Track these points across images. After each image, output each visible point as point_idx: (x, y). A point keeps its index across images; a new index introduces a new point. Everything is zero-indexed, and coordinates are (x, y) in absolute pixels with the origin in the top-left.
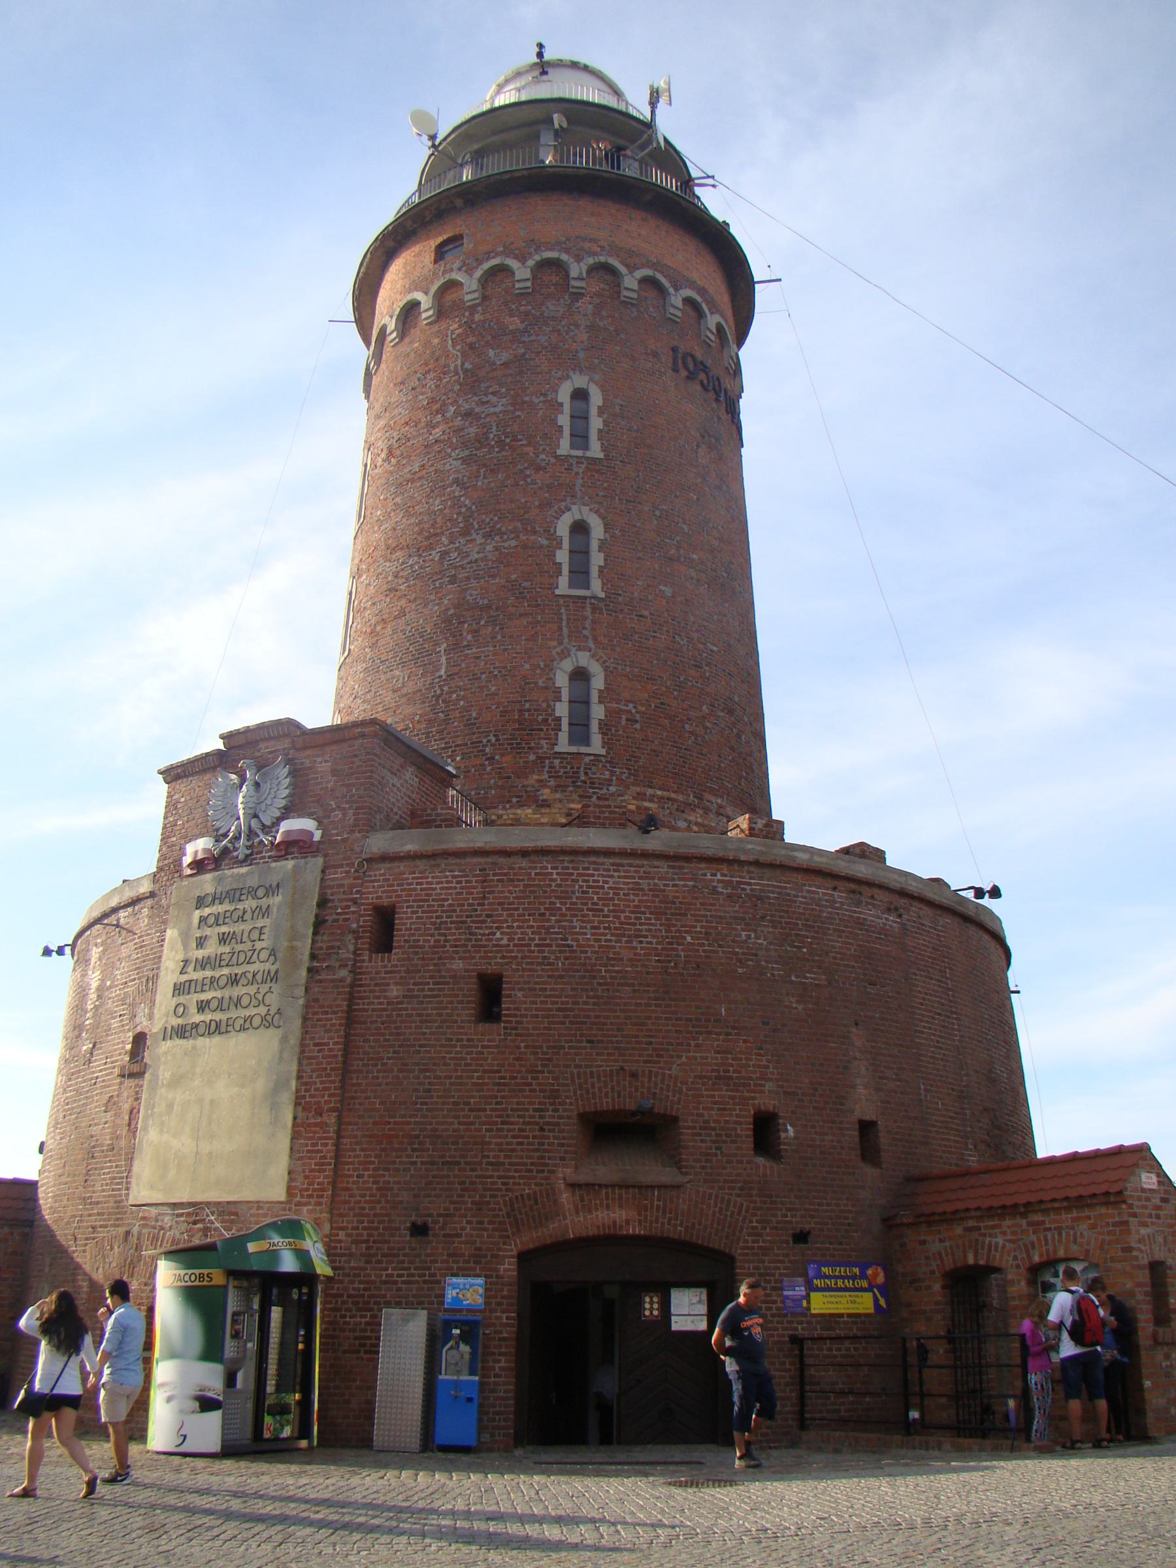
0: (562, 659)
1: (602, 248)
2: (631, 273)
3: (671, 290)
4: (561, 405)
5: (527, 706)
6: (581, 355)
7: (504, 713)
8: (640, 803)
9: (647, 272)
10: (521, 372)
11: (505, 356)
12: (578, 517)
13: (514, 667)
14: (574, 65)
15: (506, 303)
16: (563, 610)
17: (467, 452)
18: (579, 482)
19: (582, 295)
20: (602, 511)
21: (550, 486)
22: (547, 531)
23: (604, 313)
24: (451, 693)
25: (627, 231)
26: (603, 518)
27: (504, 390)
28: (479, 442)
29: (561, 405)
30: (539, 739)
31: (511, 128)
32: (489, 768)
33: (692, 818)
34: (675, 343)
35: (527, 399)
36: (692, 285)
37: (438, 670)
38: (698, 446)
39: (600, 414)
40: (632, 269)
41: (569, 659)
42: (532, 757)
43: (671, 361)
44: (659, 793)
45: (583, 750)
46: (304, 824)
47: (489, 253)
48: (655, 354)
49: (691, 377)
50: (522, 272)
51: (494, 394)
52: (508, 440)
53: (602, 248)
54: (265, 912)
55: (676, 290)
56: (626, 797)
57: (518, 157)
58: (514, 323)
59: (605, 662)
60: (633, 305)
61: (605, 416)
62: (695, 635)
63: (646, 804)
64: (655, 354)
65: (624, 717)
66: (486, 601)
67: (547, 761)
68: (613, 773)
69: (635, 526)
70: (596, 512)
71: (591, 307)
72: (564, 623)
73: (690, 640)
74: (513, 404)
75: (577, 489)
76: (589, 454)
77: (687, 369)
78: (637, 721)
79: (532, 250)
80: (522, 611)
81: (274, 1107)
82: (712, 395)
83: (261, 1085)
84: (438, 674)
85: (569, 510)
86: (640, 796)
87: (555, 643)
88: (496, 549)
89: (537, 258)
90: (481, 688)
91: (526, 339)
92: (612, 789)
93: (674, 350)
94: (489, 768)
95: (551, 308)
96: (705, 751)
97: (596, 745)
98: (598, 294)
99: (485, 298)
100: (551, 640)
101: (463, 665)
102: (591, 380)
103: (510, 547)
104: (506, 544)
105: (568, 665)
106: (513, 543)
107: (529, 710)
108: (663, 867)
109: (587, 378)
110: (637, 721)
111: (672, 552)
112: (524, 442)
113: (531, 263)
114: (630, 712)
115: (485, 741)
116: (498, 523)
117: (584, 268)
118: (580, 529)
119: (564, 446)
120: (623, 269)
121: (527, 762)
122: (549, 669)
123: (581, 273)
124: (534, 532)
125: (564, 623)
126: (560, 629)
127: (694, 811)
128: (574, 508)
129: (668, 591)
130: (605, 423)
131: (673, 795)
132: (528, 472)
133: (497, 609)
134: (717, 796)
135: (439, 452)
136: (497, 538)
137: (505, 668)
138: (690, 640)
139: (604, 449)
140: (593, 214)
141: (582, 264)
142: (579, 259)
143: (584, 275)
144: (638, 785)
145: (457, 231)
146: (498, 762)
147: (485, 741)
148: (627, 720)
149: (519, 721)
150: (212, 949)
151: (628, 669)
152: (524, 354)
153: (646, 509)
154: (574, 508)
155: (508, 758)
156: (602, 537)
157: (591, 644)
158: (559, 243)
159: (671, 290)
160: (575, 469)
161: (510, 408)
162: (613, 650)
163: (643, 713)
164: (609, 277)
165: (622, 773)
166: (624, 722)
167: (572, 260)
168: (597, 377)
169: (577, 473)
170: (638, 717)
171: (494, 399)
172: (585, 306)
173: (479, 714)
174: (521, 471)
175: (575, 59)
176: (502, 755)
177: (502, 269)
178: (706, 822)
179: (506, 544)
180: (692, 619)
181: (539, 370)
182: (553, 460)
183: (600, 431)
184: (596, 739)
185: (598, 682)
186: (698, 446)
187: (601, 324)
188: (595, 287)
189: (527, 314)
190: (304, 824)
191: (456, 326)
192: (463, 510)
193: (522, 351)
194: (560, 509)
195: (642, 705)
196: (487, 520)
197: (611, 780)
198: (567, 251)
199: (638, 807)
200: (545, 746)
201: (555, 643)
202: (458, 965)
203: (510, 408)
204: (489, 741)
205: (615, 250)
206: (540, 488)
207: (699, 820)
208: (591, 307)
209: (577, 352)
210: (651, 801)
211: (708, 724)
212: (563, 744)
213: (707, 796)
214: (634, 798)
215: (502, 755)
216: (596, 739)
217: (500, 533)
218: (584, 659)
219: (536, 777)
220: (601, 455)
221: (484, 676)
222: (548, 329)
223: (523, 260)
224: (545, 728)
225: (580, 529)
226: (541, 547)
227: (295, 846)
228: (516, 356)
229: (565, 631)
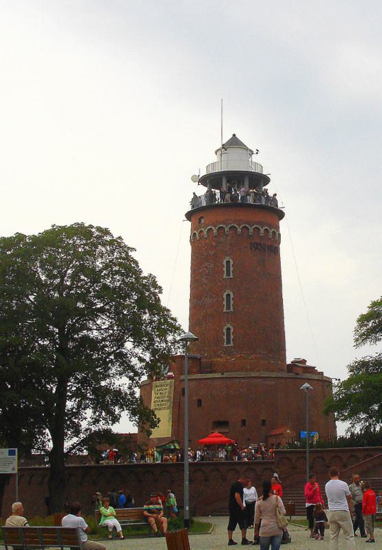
40: (239, 226)
46: (172, 374)
49: (256, 249)
54: (166, 389)
81: (169, 422)
83: (167, 418)
93: (251, 243)
105: (226, 327)
108: (227, 380)
118: (228, 295)
119: (225, 276)
120: (237, 227)
122: (222, 328)
150: (159, 395)
184: (232, 343)
185: (232, 331)
190: (172, 374)
198: (224, 224)
202: (195, 398)
205: (235, 221)
212: (225, 345)
216: (232, 343)
218: (229, 326)
223: (215, 227)
225: (228, 295)
227: (170, 377)
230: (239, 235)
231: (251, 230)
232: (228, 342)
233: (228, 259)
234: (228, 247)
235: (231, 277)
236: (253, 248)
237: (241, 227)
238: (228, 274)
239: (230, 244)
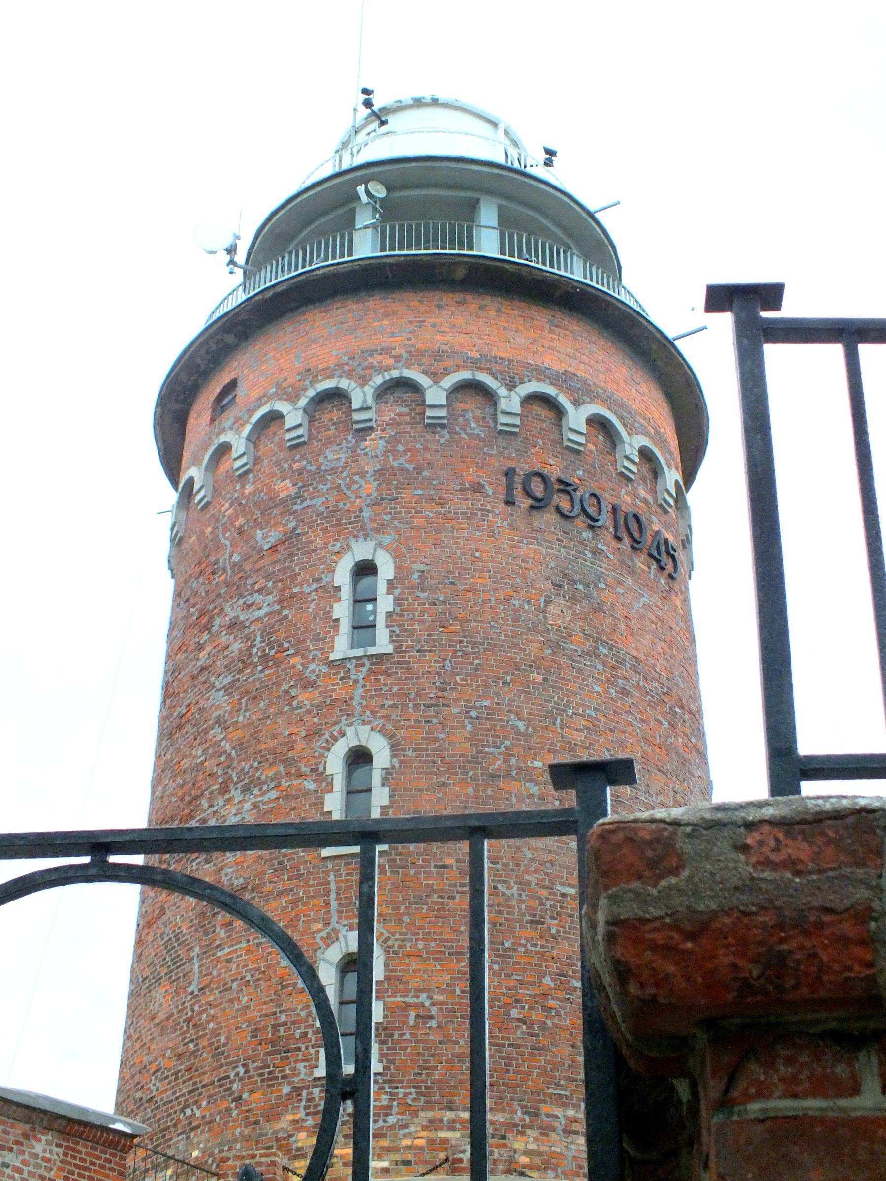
0: (328, 946)
1: (398, 358)
2: (436, 382)
3: (502, 392)
4: (338, 589)
5: (283, 1018)
6: (367, 513)
7: (254, 1034)
8: (432, 1135)
9: (465, 375)
10: (292, 555)
11: (274, 536)
12: (354, 743)
13: (269, 967)
14: (419, 103)
15: (278, 463)
16: (332, 878)
17: (230, 679)
19: (371, 428)
20: (389, 727)
21: (319, 707)
22: (314, 770)
23: (400, 448)
24: (201, 1012)
25: (434, 326)
26: (390, 736)
27: (270, 584)
28: (243, 662)
29: (338, 589)
30: (296, 1061)
31: (325, 213)
32: (235, 1113)
33: (519, 1145)
34: (510, 464)
35: (296, 590)
36: (541, 374)
37: (190, 984)
38: (548, 602)
39: (390, 591)
40: (436, 376)
41: (336, 945)
42: (286, 1089)
43: (503, 491)
47: (260, 399)
48: (477, 488)
49: (538, 505)
50: (293, 415)
51: (259, 591)
52: (272, 653)
53: (398, 358)
55: (511, 387)
56: (412, 1129)
57: (290, 264)
58: (285, 488)
59: (386, 941)
60: (443, 426)
61: (397, 592)
62: (532, 879)
63: (443, 1134)
64: (477, 488)
65: (413, 1014)
66: (241, 881)
67: (304, 1093)
68: (393, 1096)
69: (436, 739)
70: (382, 731)
71: (382, 443)
72: (333, 896)
73: (523, 885)
74: (280, 602)
75: (355, 703)
76: (372, 651)
77: (529, 494)
78: (431, 1017)
79: (307, 383)
80: (280, 886)
82: (581, 522)
84: (189, 990)
85: (343, 734)
86: (435, 1124)
87: (320, 926)
88: (255, 806)
89: (311, 393)
90: (231, 1001)
91: (296, 507)
92: (392, 1120)
93: (509, 474)
94: (235, 1113)
95: (331, 456)
96: (544, 1042)
98: (393, 423)
99: (257, 460)
100: (315, 921)
101: (215, 973)
102: (379, 545)
103: (270, 801)
104: (265, 798)
106: (274, 794)
107: (285, 1024)
109: (371, 544)
110: (431, 1017)
111: (498, 764)
112: (291, 651)
113: (303, 402)
114: (422, 1005)
115: (232, 1075)
116: (257, 769)
117: (369, 391)
118: (359, 757)
119: (342, 646)
120: (424, 381)
121: (280, 1097)
123: (365, 401)
124: (299, 775)
125: (333, 896)
126: (328, 904)
127: (522, 1133)
128: (350, 731)
130: (398, 601)
132: (293, 693)
133: (253, 890)
134: (565, 1105)
135: (204, 682)
136: (256, 791)
137: (258, 969)
138: (523, 885)
139: (394, 639)
140: (386, 315)
141: (366, 388)
142: (363, 381)
143: (370, 401)
144: (432, 1108)
145: (232, 376)
146: (248, 1103)
147: (232, 1075)
148: (417, 1017)
149: (273, 1043)
151: (421, 945)
152: (295, 529)
153: (455, 711)
154: (350, 731)
155: (257, 1096)
156: (388, 765)
158: (340, 366)
159: (502, 392)
160: (353, 677)
161: (277, 607)
162: (399, 920)
163: (442, 1003)
164: (408, 396)
165: (406, 1094)
166: (412, 1022)
167: (353, 385)
168: (387, 540)
169: (357, 681)
170: (434, 1010)
171: (257, 598)
172: (375, 444)
173: (228, 1038)
174: (287, 692)
175: (418, 96)
176: (251, 1092)
177: (275, 417)
178: (544, 1148)
179: (265, 798)
180: (529, 855)
181: (312, 546)
182: (325, 669)
183: (389, 614)
186: (548, 602)
187: (395, 464)
188: (392, 411)
189: (300, 472)
191: (227, 505)
192: (223, 758)
193: (292, 525)
194: (332, 736)
195: (441, 991)
196: (247, 767)
197: (390, 1107)
198: (350, 374)
199: (431, 1141)
200: (303, 1071)
201: (320, 926)
203: (277, 607)
204: (237, 1074)
205: (415, 356)
206: (309, 712)
207: (532, 1146)
208: (382, 443)
209: (361, 510)
210: (452, 1128)
211: (552, 1003)
213: (544, 1108)
214: (425, 1128)
215: (251, 1092)
217: (260, 783)
219: (290, 1117)
220: (390, 649)
221: (235, 985)
222: (325, 488)
224: (303, 1046)
225: (359, 757)
226: (307, 793)
228: (286, 533)
229: (334, 905)
230: (434, 426)
231: (510, 402)
233: (362, 550)
234: (369, 487)
236: (525, 503)
237: (449, 382)
238: (363, 628)
239: (383, 474)
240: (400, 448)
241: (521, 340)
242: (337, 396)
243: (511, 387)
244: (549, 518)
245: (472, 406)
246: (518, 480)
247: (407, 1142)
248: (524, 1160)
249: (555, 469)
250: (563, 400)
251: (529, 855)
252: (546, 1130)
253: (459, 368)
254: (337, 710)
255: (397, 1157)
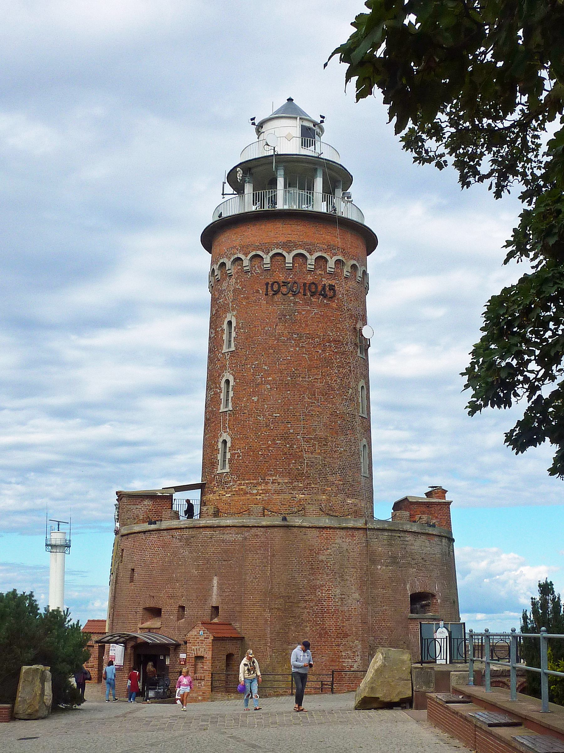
9: (254, 253)
18: (228, 362)
44: (247, 482)
45: (224, 471)
49: (276, 293)
63: (242, 487)
71: (234, 280)
93: (267, 284)
97: (227, 470)
105: (221, 440)
129: (255, 399)
131: (252, 481)
138: (264, 416)
157: (228, 430)
168: (235, 313)
185: (229, 445)
199: (239, 489)
216: (227, 466)
230: (247, 272)
231: (267, 259)
232: (224, 466)
234: (231, 294)
235: (233, 348)
236: (271, 293)
240: (238, 281)
241: (272, 234)
242: (223, 264)
243: (267, 254)
244: (280, 295)
245: (256, 262)
246: (270, 285)
247: (234, 489)
248: (261, 492)
249: (281, 277)
250: (285, 253)
251: (266, 406)
252: (267, 483)
253: (253, 250)
254: (223, 368)
255: (232, 493)
